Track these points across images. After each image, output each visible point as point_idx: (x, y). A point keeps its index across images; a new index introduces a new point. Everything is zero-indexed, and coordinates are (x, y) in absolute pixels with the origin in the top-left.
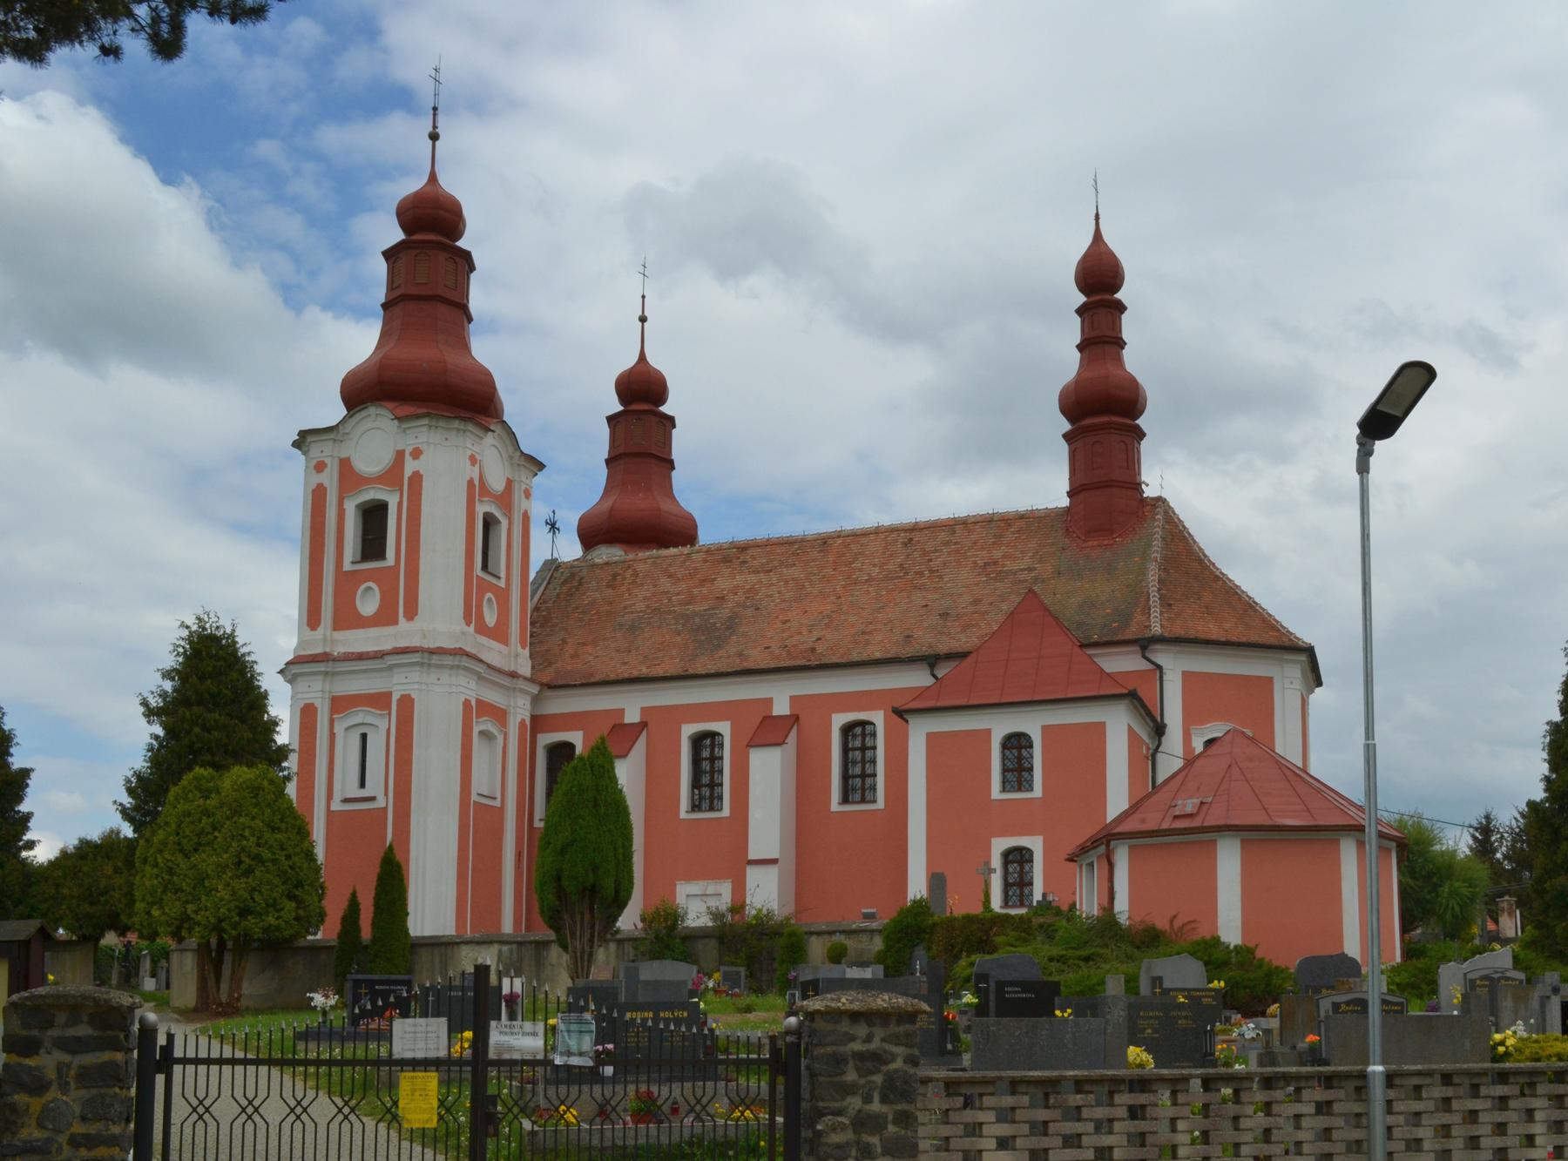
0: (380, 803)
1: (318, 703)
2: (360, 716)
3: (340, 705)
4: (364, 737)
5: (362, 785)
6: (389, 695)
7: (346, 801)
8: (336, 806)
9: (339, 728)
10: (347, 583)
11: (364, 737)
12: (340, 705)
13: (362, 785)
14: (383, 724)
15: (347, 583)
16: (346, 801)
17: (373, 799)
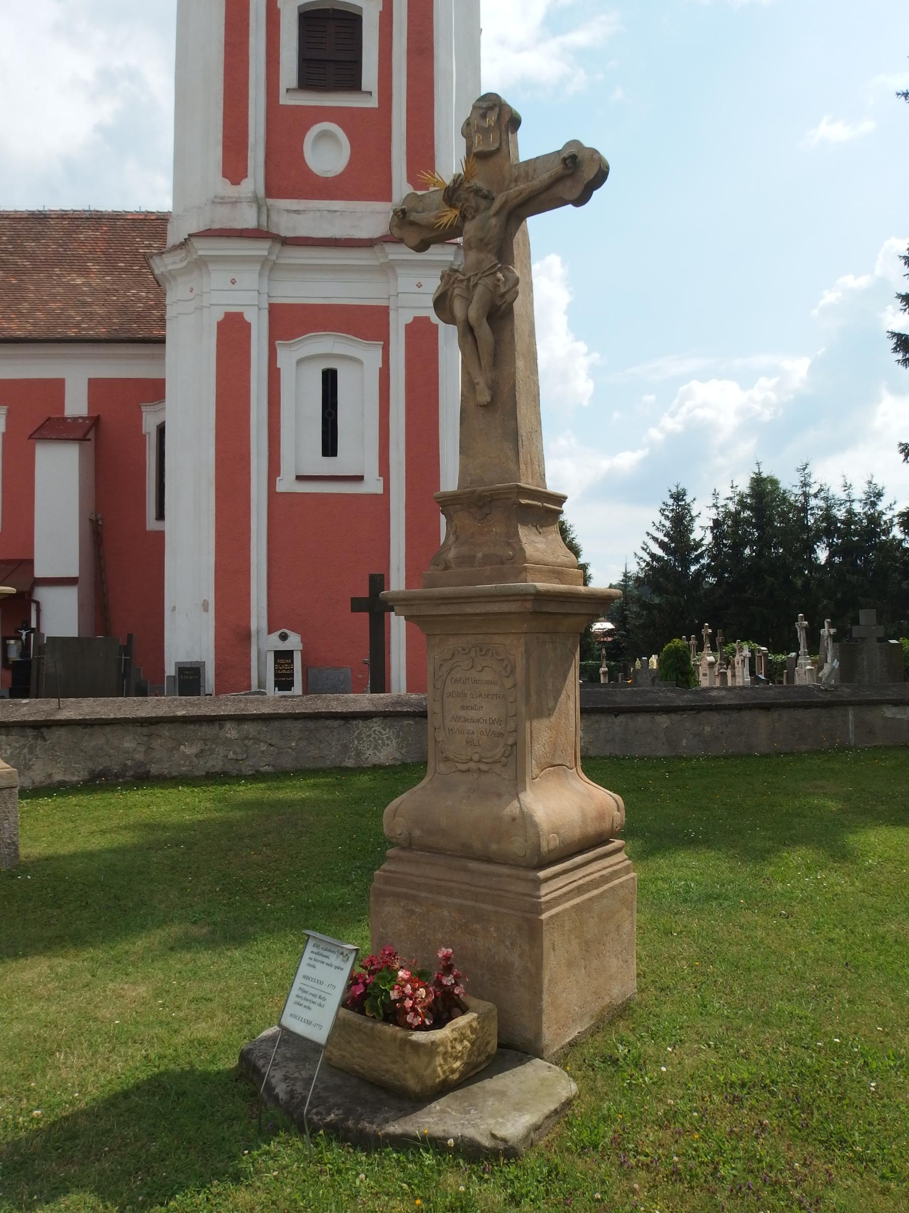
0: (372, 485)
1: (250, 316)
2: (325, 345)
3: (288, 322)
4: (330, 379)
5: (330, 447)
6: (384, 312)
7: (300, 478)
8: (286, 484)
9: (287, 358)
10: (286, 129)
11: (330, 379)
12: (288, 322)
13: (330, 447)
14: (371, 356)
15: (286, 129)
16: (300, 478)
17: (360, 478)
